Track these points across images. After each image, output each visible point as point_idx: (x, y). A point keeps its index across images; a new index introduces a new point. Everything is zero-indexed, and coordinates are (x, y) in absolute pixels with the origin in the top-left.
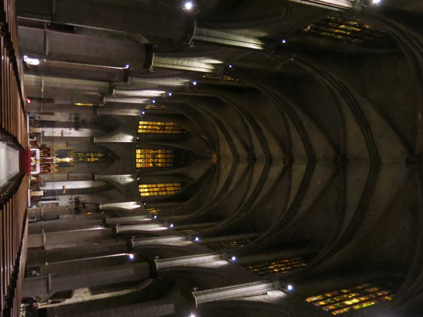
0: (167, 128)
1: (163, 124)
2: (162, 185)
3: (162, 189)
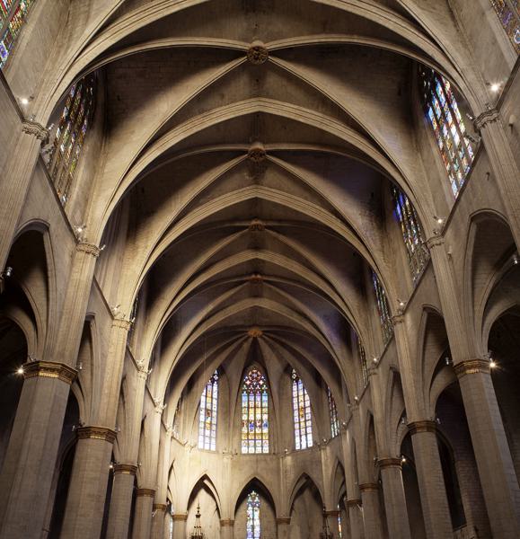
0: (209, 406)
1: (203, 412)
2: (296, 413)
3: (301, 413)
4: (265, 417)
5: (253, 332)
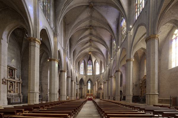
4: (92, 69)
5: (90, 53)
